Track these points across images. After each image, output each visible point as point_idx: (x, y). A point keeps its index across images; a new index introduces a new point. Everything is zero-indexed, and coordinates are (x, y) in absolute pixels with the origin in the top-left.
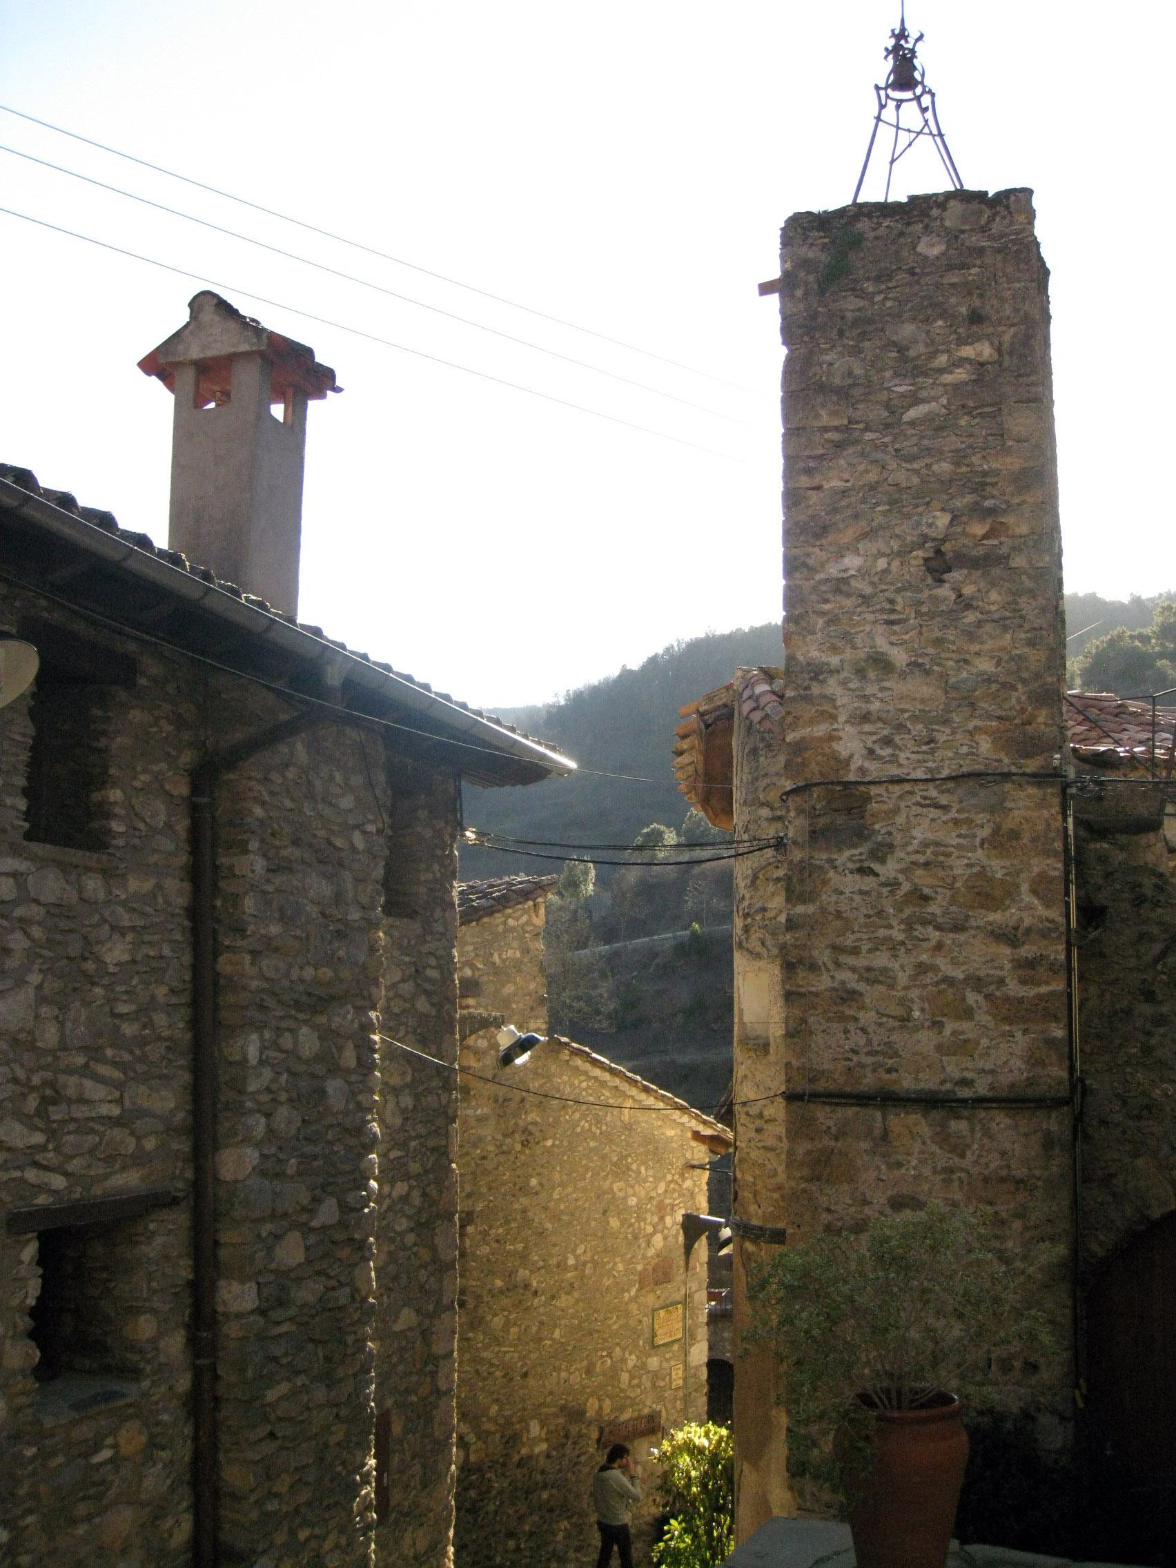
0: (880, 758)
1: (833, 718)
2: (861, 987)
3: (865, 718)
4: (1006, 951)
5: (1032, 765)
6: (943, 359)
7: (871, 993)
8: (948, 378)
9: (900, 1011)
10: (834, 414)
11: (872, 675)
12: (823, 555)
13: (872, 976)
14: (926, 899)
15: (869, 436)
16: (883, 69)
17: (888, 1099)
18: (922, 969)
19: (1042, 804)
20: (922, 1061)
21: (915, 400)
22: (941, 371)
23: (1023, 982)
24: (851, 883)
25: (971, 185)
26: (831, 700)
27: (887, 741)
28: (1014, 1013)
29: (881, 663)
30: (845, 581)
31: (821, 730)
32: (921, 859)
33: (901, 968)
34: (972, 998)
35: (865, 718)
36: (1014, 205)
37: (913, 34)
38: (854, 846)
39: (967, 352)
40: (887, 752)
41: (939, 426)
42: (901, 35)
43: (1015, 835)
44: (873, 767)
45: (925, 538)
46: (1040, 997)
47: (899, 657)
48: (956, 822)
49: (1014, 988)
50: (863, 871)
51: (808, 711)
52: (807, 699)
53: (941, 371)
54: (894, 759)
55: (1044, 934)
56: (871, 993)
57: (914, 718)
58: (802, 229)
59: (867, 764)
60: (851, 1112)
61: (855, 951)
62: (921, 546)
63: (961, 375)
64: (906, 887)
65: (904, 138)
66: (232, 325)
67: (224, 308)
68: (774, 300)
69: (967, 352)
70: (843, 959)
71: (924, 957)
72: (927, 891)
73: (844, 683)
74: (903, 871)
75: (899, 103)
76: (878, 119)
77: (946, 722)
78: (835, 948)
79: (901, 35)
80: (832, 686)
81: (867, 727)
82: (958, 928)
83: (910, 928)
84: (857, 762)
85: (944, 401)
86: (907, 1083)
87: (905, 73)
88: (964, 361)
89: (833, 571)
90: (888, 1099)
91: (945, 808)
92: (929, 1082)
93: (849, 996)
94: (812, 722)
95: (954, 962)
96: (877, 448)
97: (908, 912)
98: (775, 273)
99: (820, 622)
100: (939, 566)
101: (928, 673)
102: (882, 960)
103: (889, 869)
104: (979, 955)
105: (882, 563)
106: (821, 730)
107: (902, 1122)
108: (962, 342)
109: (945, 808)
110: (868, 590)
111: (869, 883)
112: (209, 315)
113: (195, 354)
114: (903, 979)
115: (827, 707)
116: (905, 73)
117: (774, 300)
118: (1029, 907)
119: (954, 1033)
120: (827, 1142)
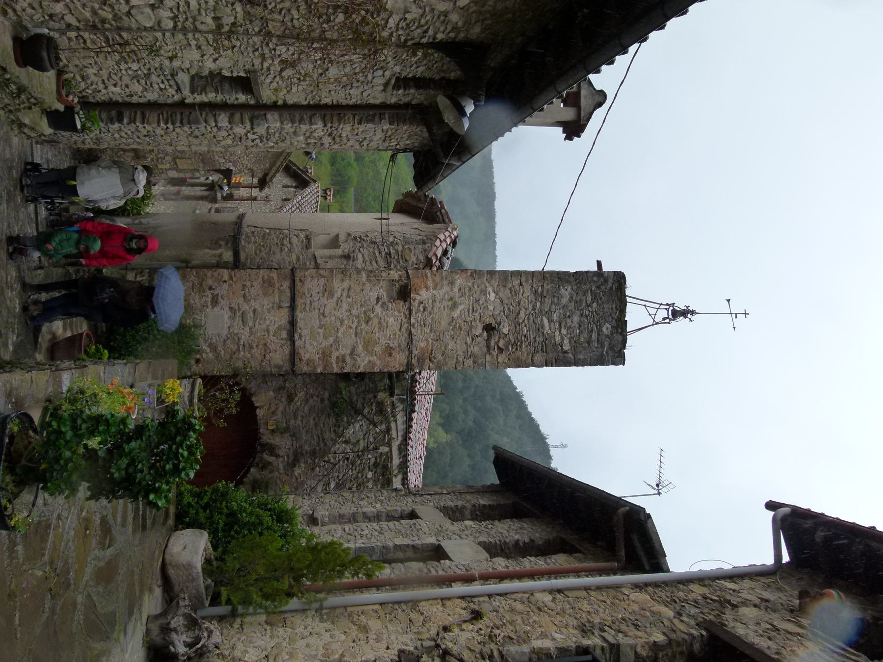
0: (419, 306)
1: (435, 289)
2: (335, 299)
3: (434, 301)
4: (349, 352)
5: (414, 361)
6: (564, 331)
7: (331, 303)
8: (557, 333)
9: (327, 313)
10: (548, 291)
11: (450, 303)
12: (495, 286)
13: (339, 301)
14: (367, 322)
15: (538, 304)
16: (681, 305)
17: (293, 308)
18: (342, 322)
19: (400, 365)
20: (306, 321)
21: (550, 321)
22: (560, 331)
23: (337, 358)
24: (373, 295)
25: (630, 339)
26: (442, 288)
27: (424, 309)
28: (325, 355)
29: (454, 306)
30: (485, 294)
31: (430, 283)
32: (382, 321)
33: (342, 313)
34: (331, 340)
35: (434, 301)
36: (618, 358)
37: (694, 317)
38: (387, 296)
39: (566, 341)
40: (422, 309)
41: (540, 329)
42: (693, 312)
43: (390, 355)
44: (416, 304)
45: (499, 324)
46: (332, 364)
47: (456, 313)
48: (395, 334)
49: (335, 355)
50: (378, 299)
51: (438, 279)
52: (442, 279)
53: (560, 331)
54: (418, 311)
55: (354, 365)
56: (331, 303)
57: (432, 319)
58: (620, 279)
59: (417, 301)
60: (289, 294)
61: (348, 296)
62: (496, 322)
63: (558, 339)
64: (372, 315)
65: (653, 311)
66: (592, 108)
67: (600, 105)
68: (595, 268)
69: (566, 341)
70: (346, 291)
71: (346, 322)
72: (370, 323)
73: (447, 293)
74: (377, 314)
75: (667, 310)
76: (661, 304)
77: (431, 330)
78: (349, 289)
79: (693, 312)
80: (446, 288)
81: (430, 301)
82: (356, 335)
83: (357, 317)
84: (418, 298)
85: (549, 332)
86: (299, 315)
87: (677, 314)
88: (562, 339)
89: (490, 289)
90: (293, 308)
91: (400, 330)
92: (300, 324)
93: (331, 294)
94: (434, 281)
95: (345, 332)
96: (533, 307)
97: (363, 316)
98: (606, 268)
99: (470, 284)
100: (489, 328)
101: (449, 324)
102: (345, 306)
103: (378, 309)
104: (348, 340)
105: (491, 308)
106: (430, 283)
107: (285, 314)
108: (570, 339)
109: (400, 330)
110: (481, 302)
111: (373, 301)
112: (598, 99)
113: (583, 92)
114: (338, 314)
115: (439, 286)
116: (677, 314)
117: (595, 268)
118: (363, 361)
119: (318, 333)
120: (277, 285)
